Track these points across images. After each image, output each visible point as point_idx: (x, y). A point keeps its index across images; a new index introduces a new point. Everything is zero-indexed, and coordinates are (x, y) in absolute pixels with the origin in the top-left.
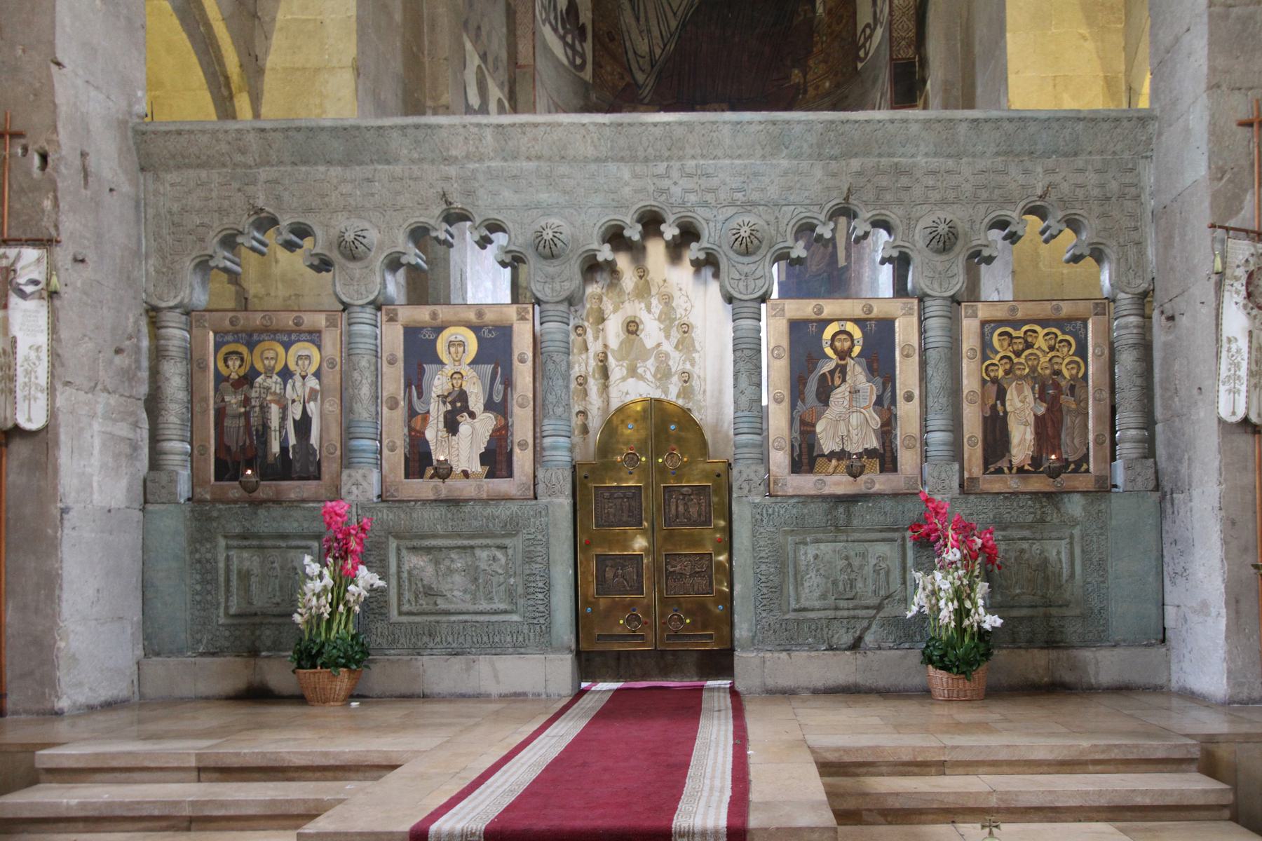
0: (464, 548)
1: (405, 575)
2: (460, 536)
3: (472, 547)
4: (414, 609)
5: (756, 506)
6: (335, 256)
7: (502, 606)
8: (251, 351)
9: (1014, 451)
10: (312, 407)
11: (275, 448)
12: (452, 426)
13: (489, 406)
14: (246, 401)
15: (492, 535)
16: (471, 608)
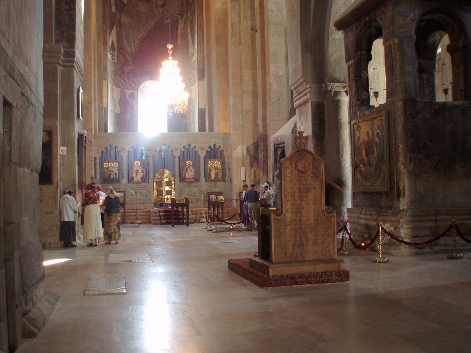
0: (139, 190)
1: (131, 193)
2: (139, 188)
3: (140, 190)
4: (132, 198)
5: (178, 184)
6: (121, 150)
7: (144, 197)
8: (108, 164)
9: (212, 177)
10: (117, 172)
11: (112, 177)
12: (137, 174)
13: (142, 172)
14: (108, 171)
15: (143, 188)
16: (140, 197)
